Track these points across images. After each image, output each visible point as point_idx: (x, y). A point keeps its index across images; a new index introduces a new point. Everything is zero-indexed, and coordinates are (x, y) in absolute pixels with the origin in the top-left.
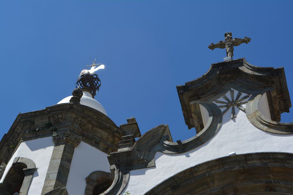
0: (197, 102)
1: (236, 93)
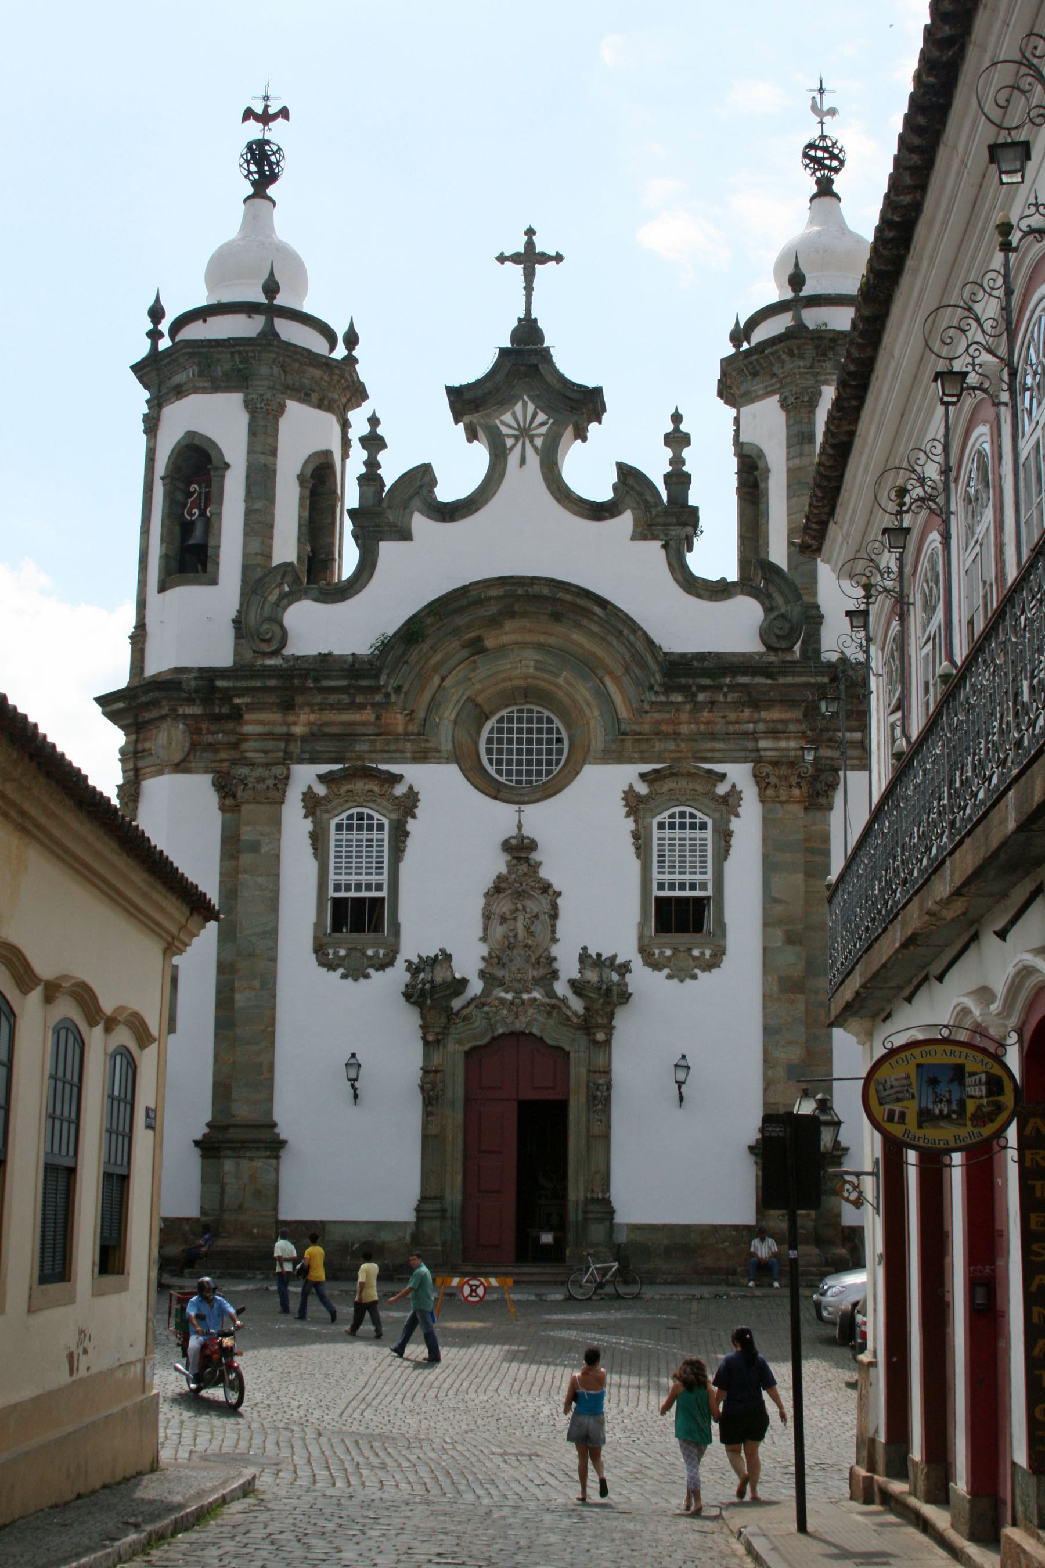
1: (531, 407)
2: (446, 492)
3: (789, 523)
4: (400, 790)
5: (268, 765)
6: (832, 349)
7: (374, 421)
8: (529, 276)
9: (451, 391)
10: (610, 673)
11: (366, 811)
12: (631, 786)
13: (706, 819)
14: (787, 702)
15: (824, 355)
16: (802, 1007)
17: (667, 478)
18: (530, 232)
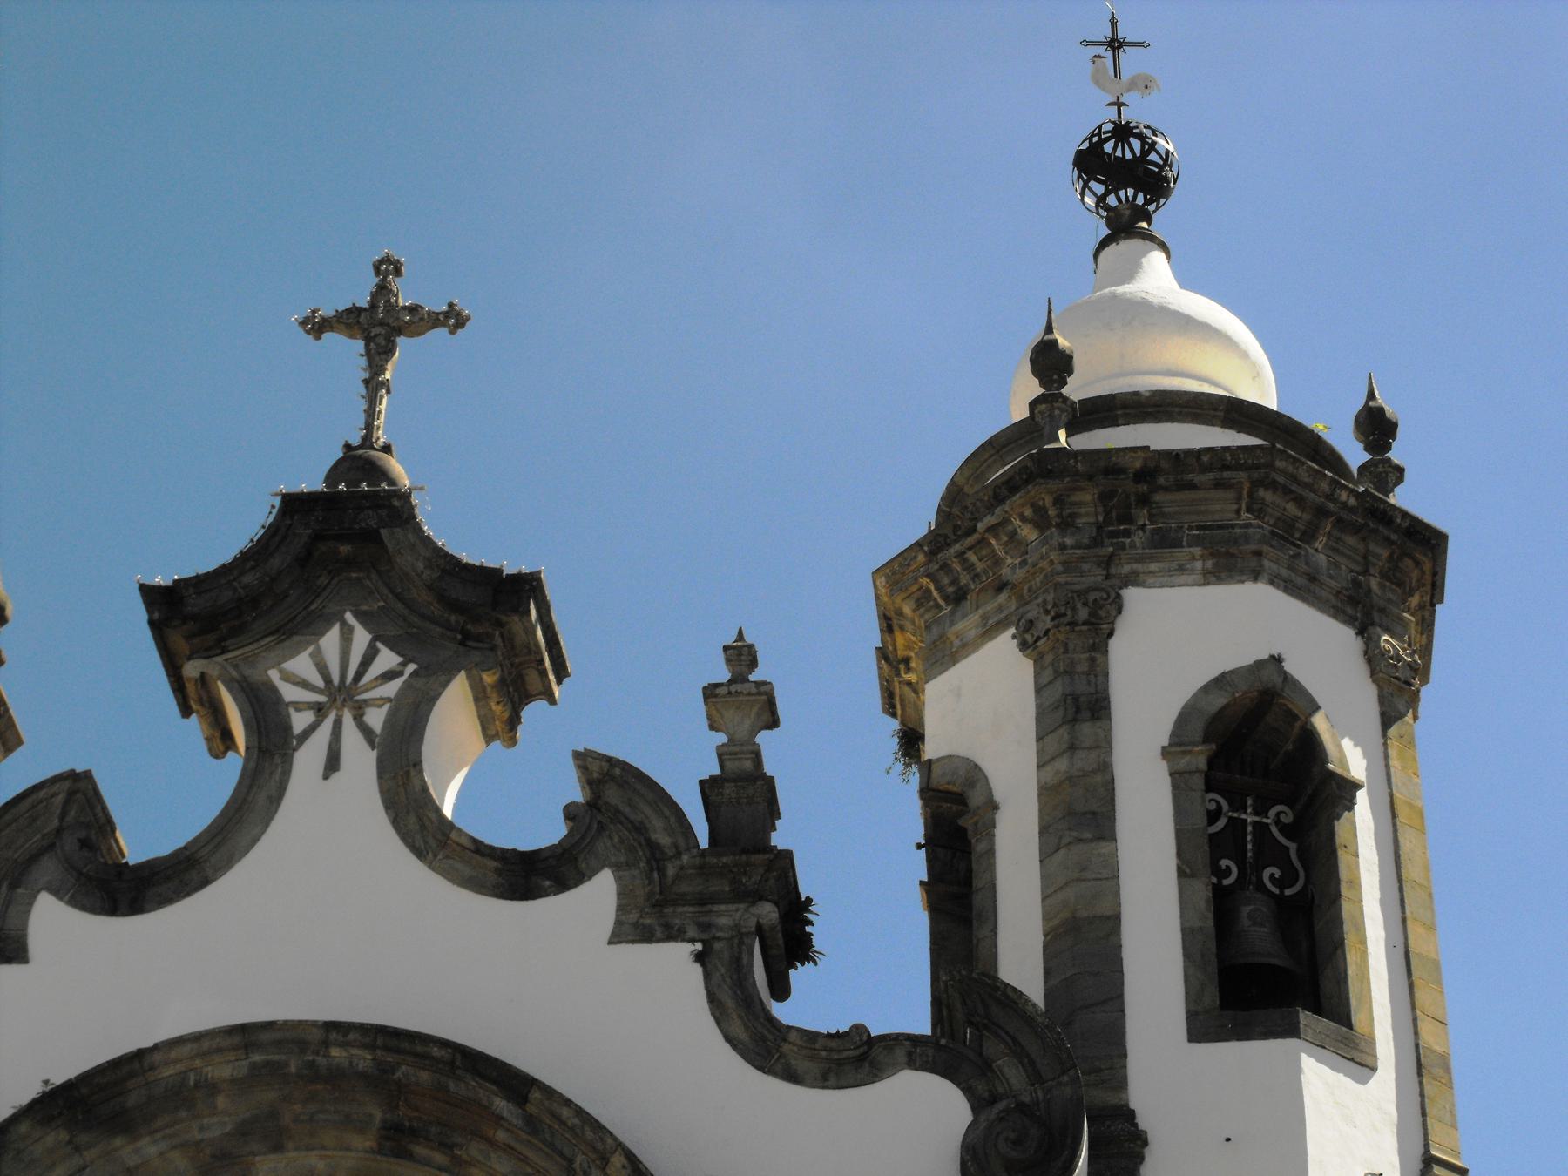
0: (211, 667)
1: (362, 638)
3: (1046, 917)
6: (1144, 500)
9: (150, 594)
15: (1129, 519)
17: (708, 788)
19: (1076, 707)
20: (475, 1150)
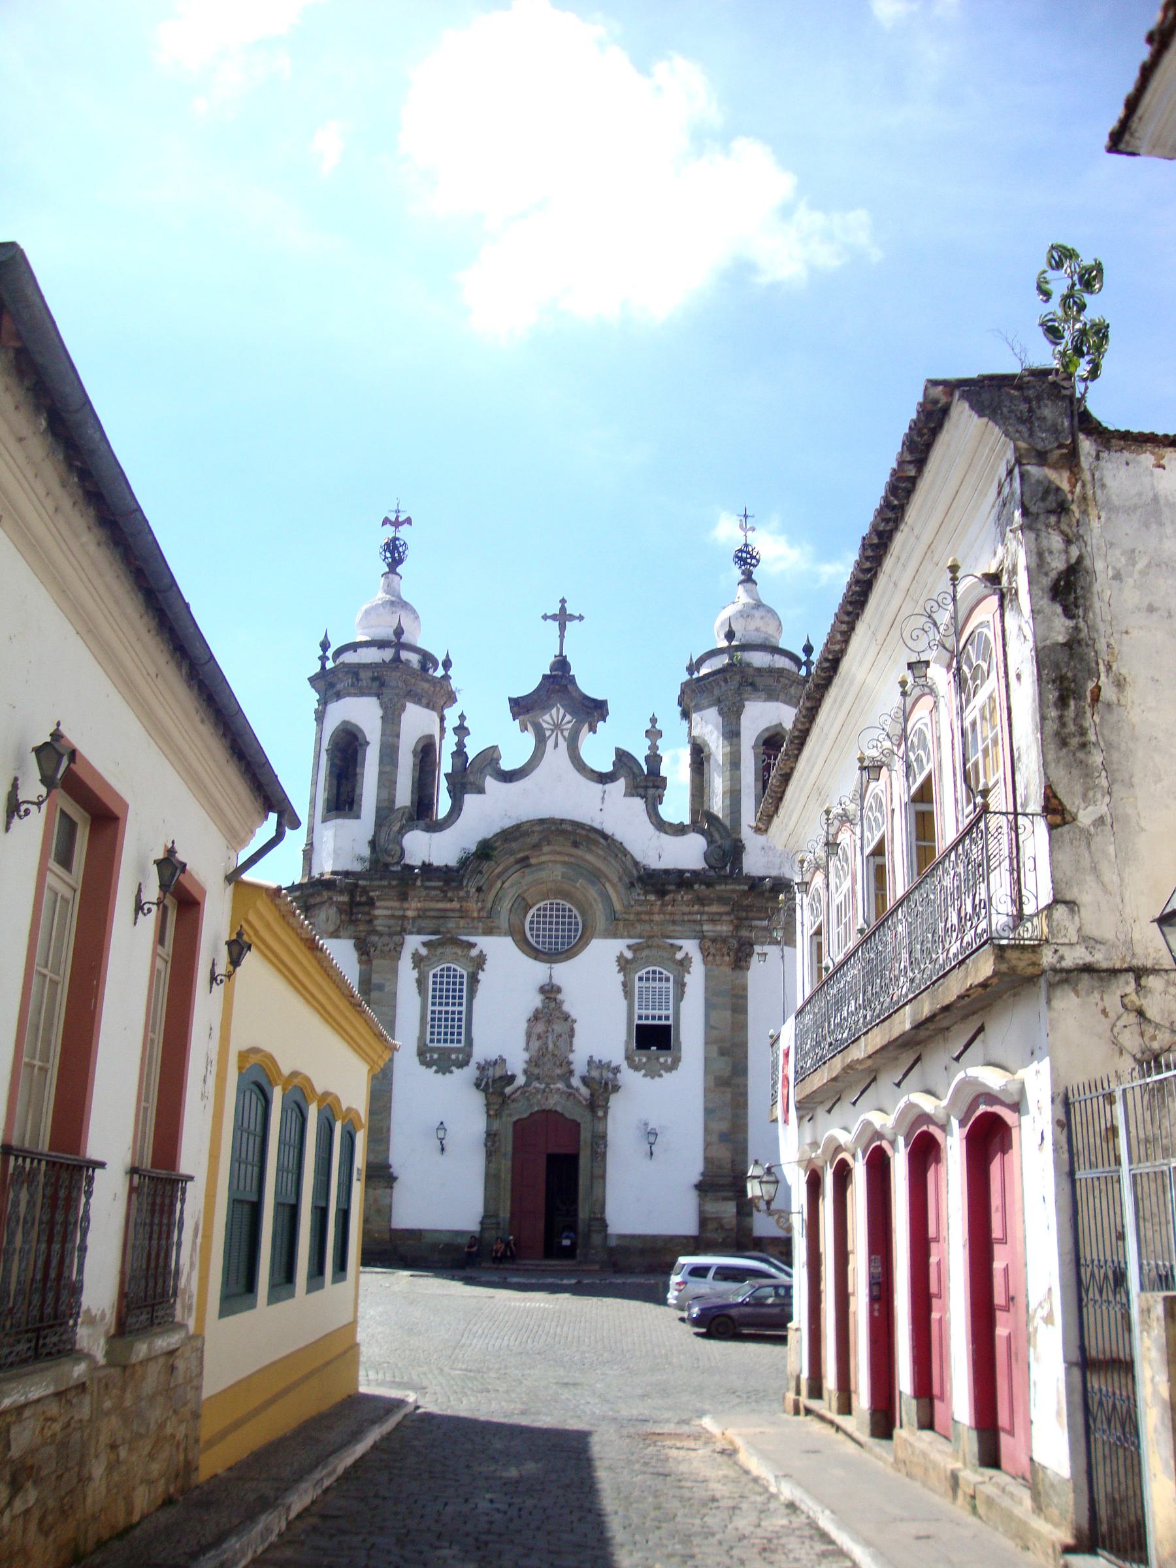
1: (562, 711)
2: (508, 763)
4: (474, 953)
5: (391, 935)
7: (462, 717)
8: (562, 628)
10: (609, 881)
11: (453, 966)
12: (621, 953)
13: (669, 975)
14: (721, 900)
16: (729, 1096)
17: (647, 758)
18: (563, 601)
19: (732, 734)
20: (594, 848)
